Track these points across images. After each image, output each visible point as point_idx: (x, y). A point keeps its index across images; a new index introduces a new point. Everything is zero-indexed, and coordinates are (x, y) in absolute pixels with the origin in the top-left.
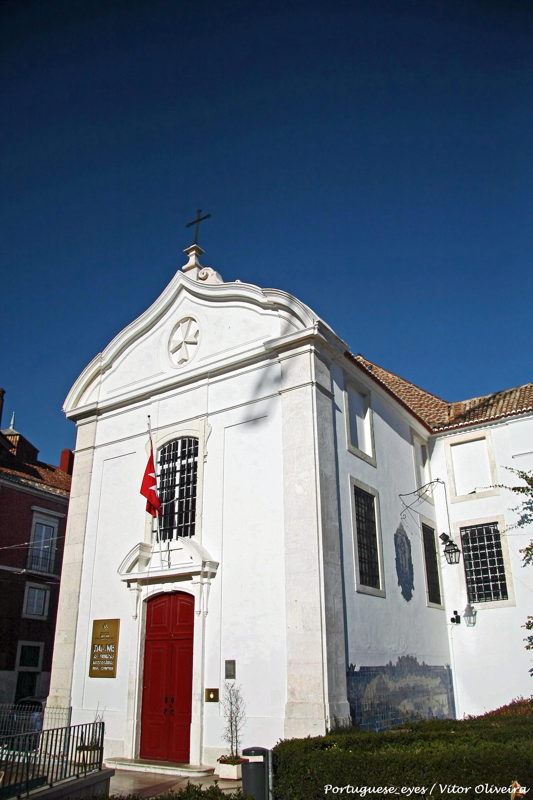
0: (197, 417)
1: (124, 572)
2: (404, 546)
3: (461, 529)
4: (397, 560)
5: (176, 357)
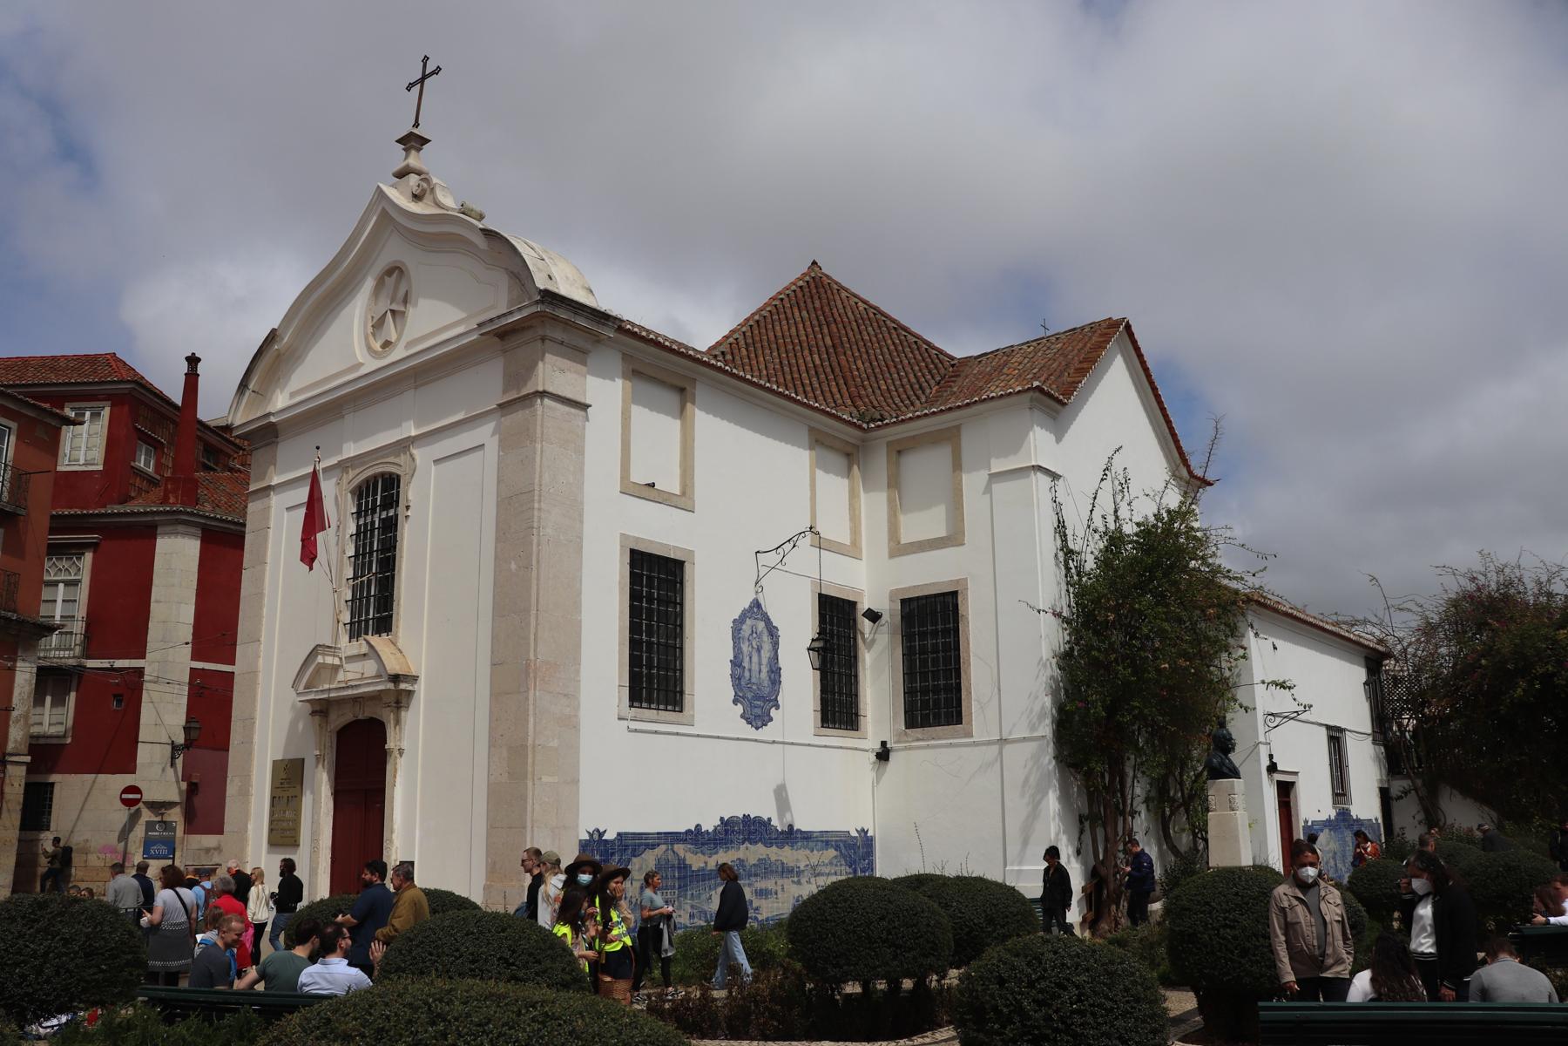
1: (301, 689)
2: (759, 636)
4: (736, 663)
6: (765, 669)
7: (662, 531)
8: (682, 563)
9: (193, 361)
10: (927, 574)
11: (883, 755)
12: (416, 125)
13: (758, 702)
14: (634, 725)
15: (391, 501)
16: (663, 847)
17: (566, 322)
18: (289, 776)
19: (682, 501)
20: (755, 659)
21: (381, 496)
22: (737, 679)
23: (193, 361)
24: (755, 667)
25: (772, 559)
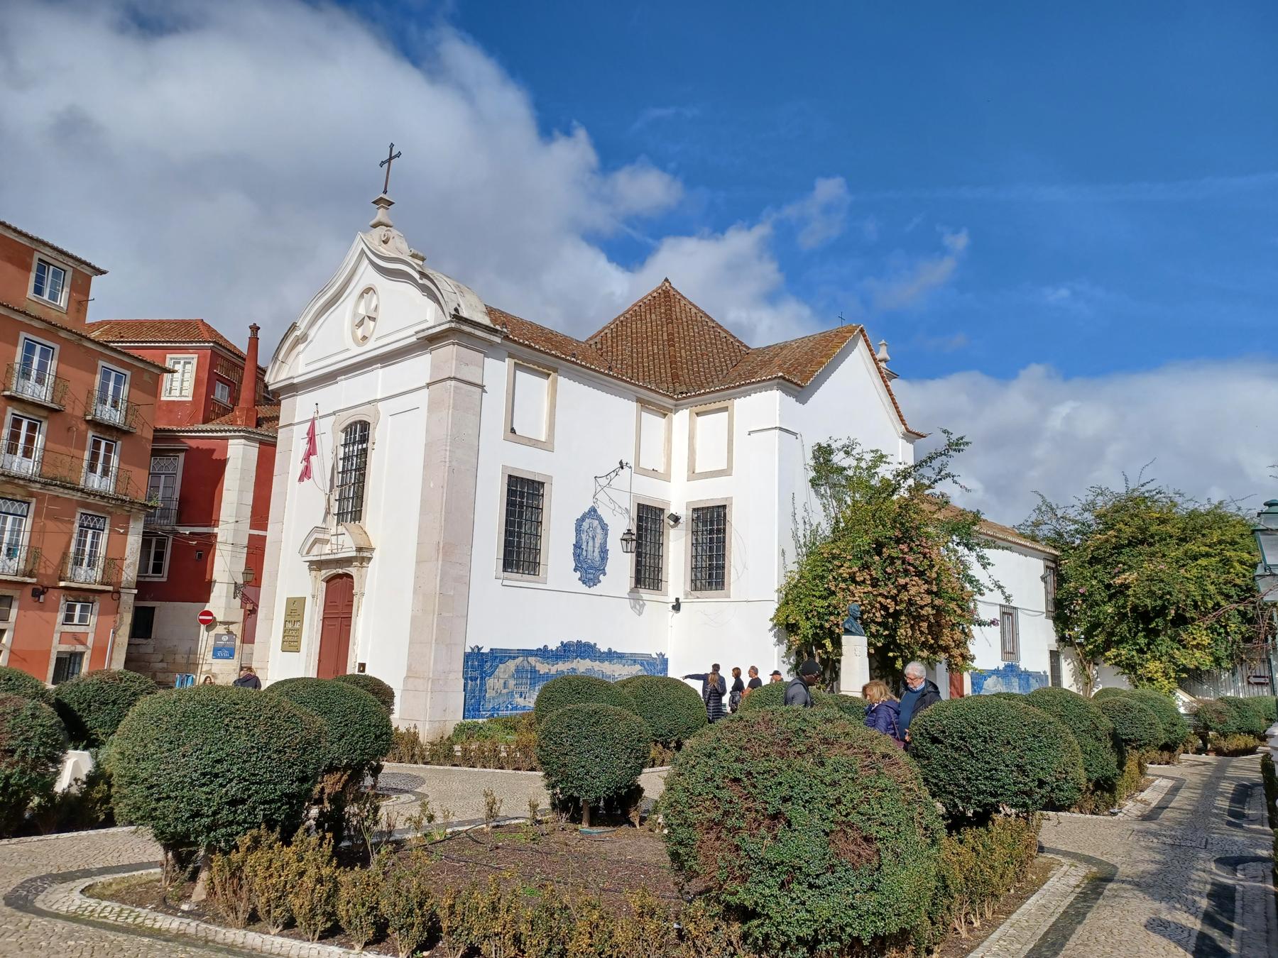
0: (369, 403)
2: (594, 529)
3: (694, 510)
4: (577, 546)
5: (360, 333)
6: (597, 551)
7: (529, 464)
8: (543, 484)
9: (255, 329)
10: (708, 493)
11: (677, 607)
12: (385, 192)
13: (590, 569)
14: (506, 582)
15: (364, 439)
16: (521, 659)
17: (470, 334)
18: (295, 609)
19: (547, 446)
20: (591, 543)
21: (359, 433)
22: (577, 556)
23: (255, 329)
24: (590, 549)
25: (603, 482)
